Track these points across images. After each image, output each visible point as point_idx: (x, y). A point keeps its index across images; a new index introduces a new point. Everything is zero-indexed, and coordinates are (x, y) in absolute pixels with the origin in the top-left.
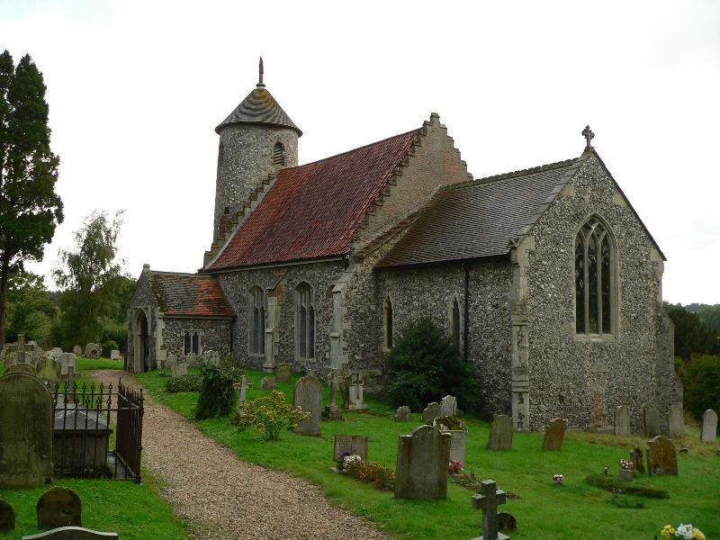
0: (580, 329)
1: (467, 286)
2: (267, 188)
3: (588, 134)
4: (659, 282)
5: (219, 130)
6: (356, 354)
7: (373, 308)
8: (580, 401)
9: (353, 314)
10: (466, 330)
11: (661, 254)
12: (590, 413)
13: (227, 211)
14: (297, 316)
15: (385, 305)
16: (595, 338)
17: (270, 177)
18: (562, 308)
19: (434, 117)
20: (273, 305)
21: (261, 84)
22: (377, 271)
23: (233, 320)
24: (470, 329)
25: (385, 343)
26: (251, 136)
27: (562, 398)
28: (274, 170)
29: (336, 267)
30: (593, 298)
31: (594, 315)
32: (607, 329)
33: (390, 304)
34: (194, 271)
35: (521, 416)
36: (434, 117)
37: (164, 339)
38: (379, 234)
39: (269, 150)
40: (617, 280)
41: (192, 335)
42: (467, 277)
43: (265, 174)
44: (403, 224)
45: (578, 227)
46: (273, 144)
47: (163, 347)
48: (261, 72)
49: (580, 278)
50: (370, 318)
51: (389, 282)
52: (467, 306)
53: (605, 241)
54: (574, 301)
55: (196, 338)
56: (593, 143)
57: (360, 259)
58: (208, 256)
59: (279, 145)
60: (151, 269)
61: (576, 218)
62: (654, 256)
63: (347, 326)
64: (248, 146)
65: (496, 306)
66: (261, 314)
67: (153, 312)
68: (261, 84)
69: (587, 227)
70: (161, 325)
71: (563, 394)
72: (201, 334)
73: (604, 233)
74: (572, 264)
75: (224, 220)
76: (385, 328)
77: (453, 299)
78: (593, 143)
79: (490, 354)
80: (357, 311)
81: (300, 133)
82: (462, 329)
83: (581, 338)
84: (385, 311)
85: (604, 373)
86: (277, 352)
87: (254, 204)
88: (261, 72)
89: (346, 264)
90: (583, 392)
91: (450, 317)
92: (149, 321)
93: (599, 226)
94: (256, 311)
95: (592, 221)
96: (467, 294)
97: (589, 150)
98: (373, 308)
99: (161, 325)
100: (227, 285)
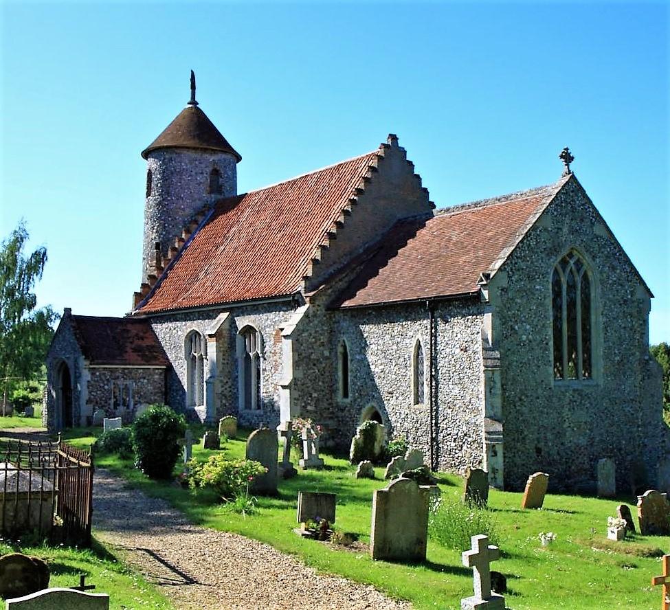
3: (567, 157)
5: (146, 154)
7: (327, 353)
8: (558, 454)
12: (570, 467)
15: (340, 349)
21: (193, 102)
25: (341, 392)
27: (539, 451)
33: (345, 347)
34: (121, 315)
37: (90, 392)
38: (331, 270)
39: (204, 179)
45: (555, 261)
48: (193, 87)
49: (557, 319)
50: (324, 365)
51: (345, 324)
54: (551, 343)
60: (73, 313)
61: (554, 250)
62: (639, 294)
64: (180, 173)
67: (76, 361)
68: (193, 102)
69: (564, 263)
71: (541, 445)
74: (549, 302)
76: (340, 374)
77: (414, 343)
80: (308, 357)
84: (340, 357)
85: (585, 423)
88: (193, 87)
98: (327, 353)
99: (86, 375)
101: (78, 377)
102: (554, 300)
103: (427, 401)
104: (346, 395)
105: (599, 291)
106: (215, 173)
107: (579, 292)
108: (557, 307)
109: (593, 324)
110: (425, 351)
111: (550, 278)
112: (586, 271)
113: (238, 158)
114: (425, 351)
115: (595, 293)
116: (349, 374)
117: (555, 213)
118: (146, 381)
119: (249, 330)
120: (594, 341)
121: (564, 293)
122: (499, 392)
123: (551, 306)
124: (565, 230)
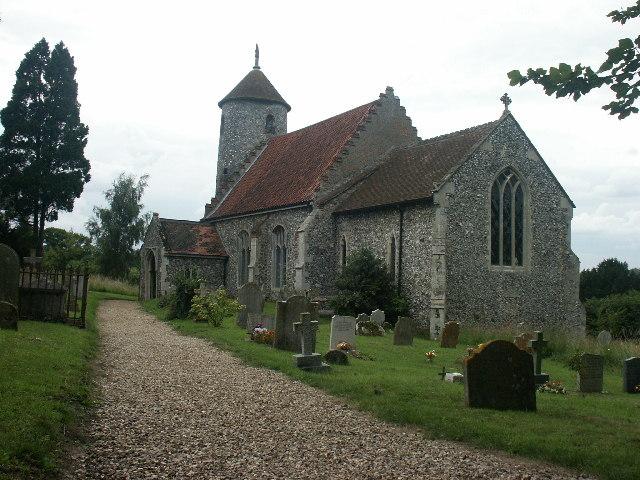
0: (495, 261)
1: (402, 225)
2: (259, 153)
3: (506, 100)
4: (568, 225)
5: (221, 104)
9: (314, 250)
10: (401, 260)
11: (571, 203)
13: (225, 171)
15: (341, 243)
16: (508, 269)
17: (262, 144)
18: (478, 243)
19: (390, 90)
20: (254, 244)
21: (257, 67)
22: (336, 215)
23: (227, 259)
24: (403, 260)
26: (246, 110)
28: (264, 137)
30: (507, 237)
31: (507, 252)
32: (520, 263)
33: (344, 240)
35: (437, 328)
36: (390, 90)
40: (528, 222)
42: (402, 215)
45: (494, 176)
46: (265, 116)
47: (167, 280)
48: (257, 56)
49: (495, 219)
52: (401, 241)
53: (519, 190)
54: (489, 237)
56: (511, 107)
58: (208, 207)
59: (270, 118)
61: (493, 168)
62: (564, 204)
65: (422, 241)
66: (246, 253)
68: (257, 67)
69: (502, 178)
70: (166, 262)
73: (518, 183)
74: (488, 206)
75: (225, 178)
78: (511, 107)
79: (418, 280)
81: (288, 108)
82: (397, 261)
83: (496, 268)
88: (257, 56)
89: (310, 209)
90: (496, 313)
91: (389, 250)
92: (156, 261)
93: (514, 176)
95: (508, 173)
96: (402, 231)
97: (507, 115)
100: (222, 230)
102: (493, 207)
105: (530, 200)
106: (270, 118)
107: (514, 201)
108: (495, 211)
109: (525, 226)
110: (397, 243)
112: (519, 186)
113: (288, 108)
114: (397, 243)
115: (527, 201)
119: (279, 230)
120: (524, 240)
121: (501, 202)
122: (444, 270)
123: (490, 210)
124: (503, 153)
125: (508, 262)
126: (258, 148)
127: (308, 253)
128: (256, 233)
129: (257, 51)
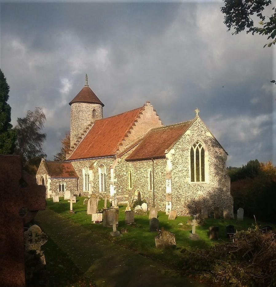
2: (90, 128)
6: (119, 190)
14: (100, 177)
15: (129, 172)
16: (198, 183)
25: (130, 186)
28: (93, 121)
29: (112, 159)
32: (203, 180)
35: (169, 209)
39: (91, 113)
41: (61, 184)
43: (89, 123)
44: (142, 139)
55: (63, 186)
57: (120, 156)
63: (116, 180)
65: (162, 173)
66: (87, 176)
69: (195, 146)
72: (65, 184)
74: (189, 158)
86: (93, 190)
87: (86, 134)
91: (149, 176)
92: (45, 179)
94: (86, 175)
95: (197, 143)
96: (154, 169)
101: (47, 182)
103: (152, 189)
104: (131, 187)
110: (152, 174)
111: (190, 151)
116: (132, 180)
117: (192, 130)
118: (70, 182)
125: (198, 180)
126: (90, 125)
127: (115, 177)
128: (91, 167)
129: (87, 76)
